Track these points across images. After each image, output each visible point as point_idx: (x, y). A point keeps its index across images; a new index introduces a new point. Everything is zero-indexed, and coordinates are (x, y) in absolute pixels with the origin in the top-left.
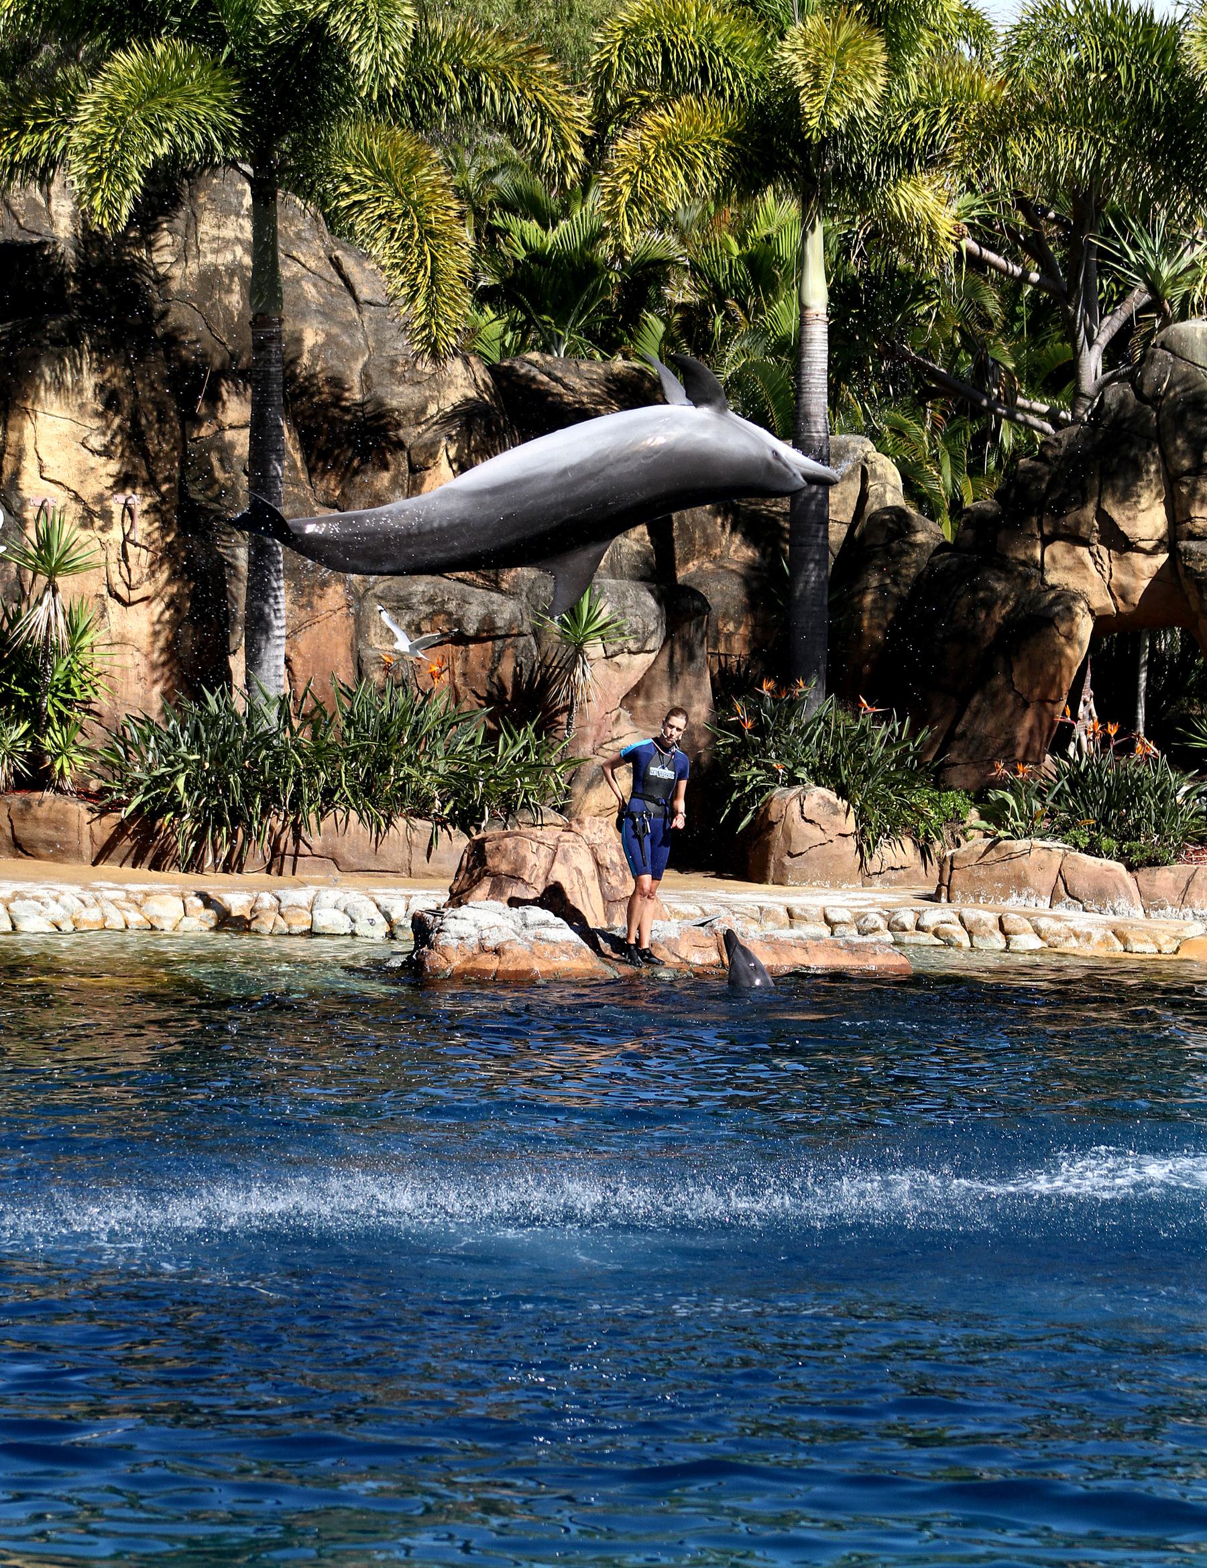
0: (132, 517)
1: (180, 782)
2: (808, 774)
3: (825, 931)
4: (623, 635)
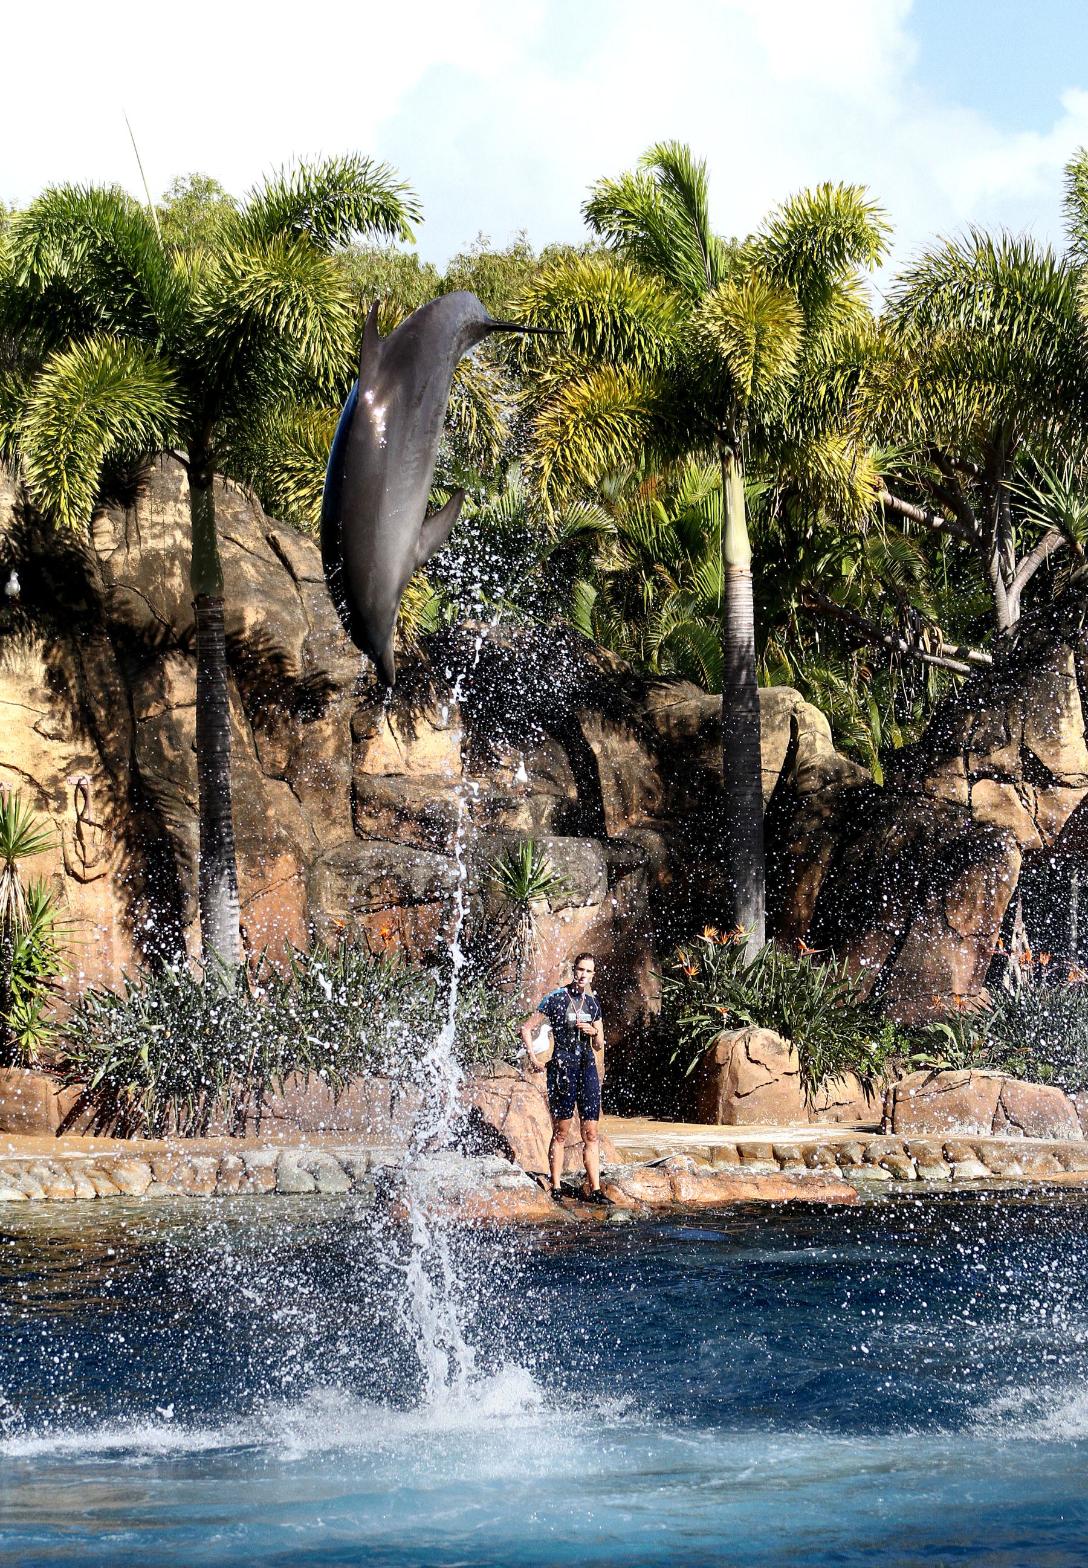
0: (85, 797)
1: (144, 1053)
2: (750, 1014)
3: (776, 1168)
4: (566, 890)
